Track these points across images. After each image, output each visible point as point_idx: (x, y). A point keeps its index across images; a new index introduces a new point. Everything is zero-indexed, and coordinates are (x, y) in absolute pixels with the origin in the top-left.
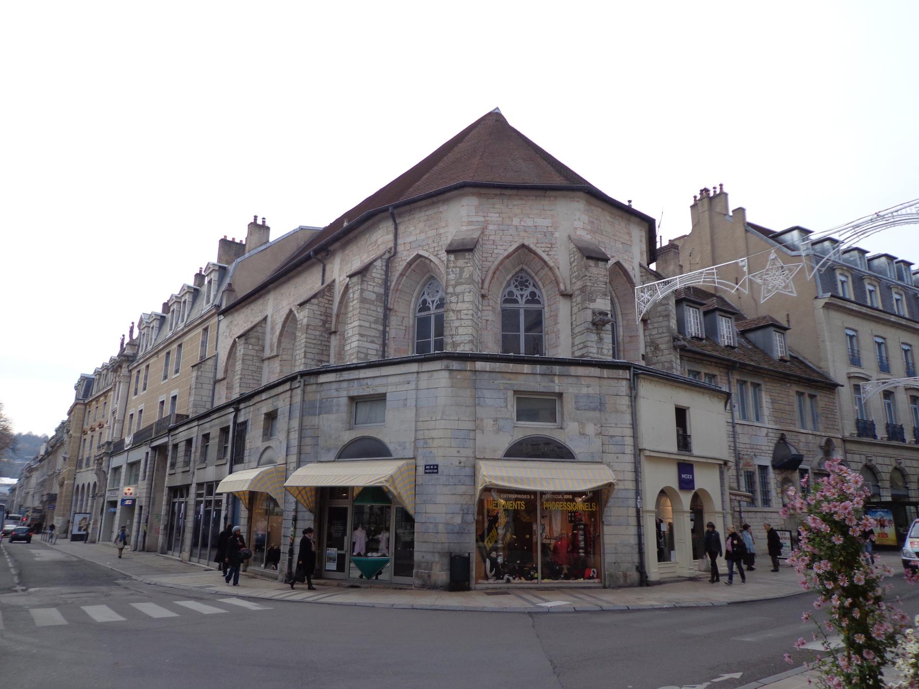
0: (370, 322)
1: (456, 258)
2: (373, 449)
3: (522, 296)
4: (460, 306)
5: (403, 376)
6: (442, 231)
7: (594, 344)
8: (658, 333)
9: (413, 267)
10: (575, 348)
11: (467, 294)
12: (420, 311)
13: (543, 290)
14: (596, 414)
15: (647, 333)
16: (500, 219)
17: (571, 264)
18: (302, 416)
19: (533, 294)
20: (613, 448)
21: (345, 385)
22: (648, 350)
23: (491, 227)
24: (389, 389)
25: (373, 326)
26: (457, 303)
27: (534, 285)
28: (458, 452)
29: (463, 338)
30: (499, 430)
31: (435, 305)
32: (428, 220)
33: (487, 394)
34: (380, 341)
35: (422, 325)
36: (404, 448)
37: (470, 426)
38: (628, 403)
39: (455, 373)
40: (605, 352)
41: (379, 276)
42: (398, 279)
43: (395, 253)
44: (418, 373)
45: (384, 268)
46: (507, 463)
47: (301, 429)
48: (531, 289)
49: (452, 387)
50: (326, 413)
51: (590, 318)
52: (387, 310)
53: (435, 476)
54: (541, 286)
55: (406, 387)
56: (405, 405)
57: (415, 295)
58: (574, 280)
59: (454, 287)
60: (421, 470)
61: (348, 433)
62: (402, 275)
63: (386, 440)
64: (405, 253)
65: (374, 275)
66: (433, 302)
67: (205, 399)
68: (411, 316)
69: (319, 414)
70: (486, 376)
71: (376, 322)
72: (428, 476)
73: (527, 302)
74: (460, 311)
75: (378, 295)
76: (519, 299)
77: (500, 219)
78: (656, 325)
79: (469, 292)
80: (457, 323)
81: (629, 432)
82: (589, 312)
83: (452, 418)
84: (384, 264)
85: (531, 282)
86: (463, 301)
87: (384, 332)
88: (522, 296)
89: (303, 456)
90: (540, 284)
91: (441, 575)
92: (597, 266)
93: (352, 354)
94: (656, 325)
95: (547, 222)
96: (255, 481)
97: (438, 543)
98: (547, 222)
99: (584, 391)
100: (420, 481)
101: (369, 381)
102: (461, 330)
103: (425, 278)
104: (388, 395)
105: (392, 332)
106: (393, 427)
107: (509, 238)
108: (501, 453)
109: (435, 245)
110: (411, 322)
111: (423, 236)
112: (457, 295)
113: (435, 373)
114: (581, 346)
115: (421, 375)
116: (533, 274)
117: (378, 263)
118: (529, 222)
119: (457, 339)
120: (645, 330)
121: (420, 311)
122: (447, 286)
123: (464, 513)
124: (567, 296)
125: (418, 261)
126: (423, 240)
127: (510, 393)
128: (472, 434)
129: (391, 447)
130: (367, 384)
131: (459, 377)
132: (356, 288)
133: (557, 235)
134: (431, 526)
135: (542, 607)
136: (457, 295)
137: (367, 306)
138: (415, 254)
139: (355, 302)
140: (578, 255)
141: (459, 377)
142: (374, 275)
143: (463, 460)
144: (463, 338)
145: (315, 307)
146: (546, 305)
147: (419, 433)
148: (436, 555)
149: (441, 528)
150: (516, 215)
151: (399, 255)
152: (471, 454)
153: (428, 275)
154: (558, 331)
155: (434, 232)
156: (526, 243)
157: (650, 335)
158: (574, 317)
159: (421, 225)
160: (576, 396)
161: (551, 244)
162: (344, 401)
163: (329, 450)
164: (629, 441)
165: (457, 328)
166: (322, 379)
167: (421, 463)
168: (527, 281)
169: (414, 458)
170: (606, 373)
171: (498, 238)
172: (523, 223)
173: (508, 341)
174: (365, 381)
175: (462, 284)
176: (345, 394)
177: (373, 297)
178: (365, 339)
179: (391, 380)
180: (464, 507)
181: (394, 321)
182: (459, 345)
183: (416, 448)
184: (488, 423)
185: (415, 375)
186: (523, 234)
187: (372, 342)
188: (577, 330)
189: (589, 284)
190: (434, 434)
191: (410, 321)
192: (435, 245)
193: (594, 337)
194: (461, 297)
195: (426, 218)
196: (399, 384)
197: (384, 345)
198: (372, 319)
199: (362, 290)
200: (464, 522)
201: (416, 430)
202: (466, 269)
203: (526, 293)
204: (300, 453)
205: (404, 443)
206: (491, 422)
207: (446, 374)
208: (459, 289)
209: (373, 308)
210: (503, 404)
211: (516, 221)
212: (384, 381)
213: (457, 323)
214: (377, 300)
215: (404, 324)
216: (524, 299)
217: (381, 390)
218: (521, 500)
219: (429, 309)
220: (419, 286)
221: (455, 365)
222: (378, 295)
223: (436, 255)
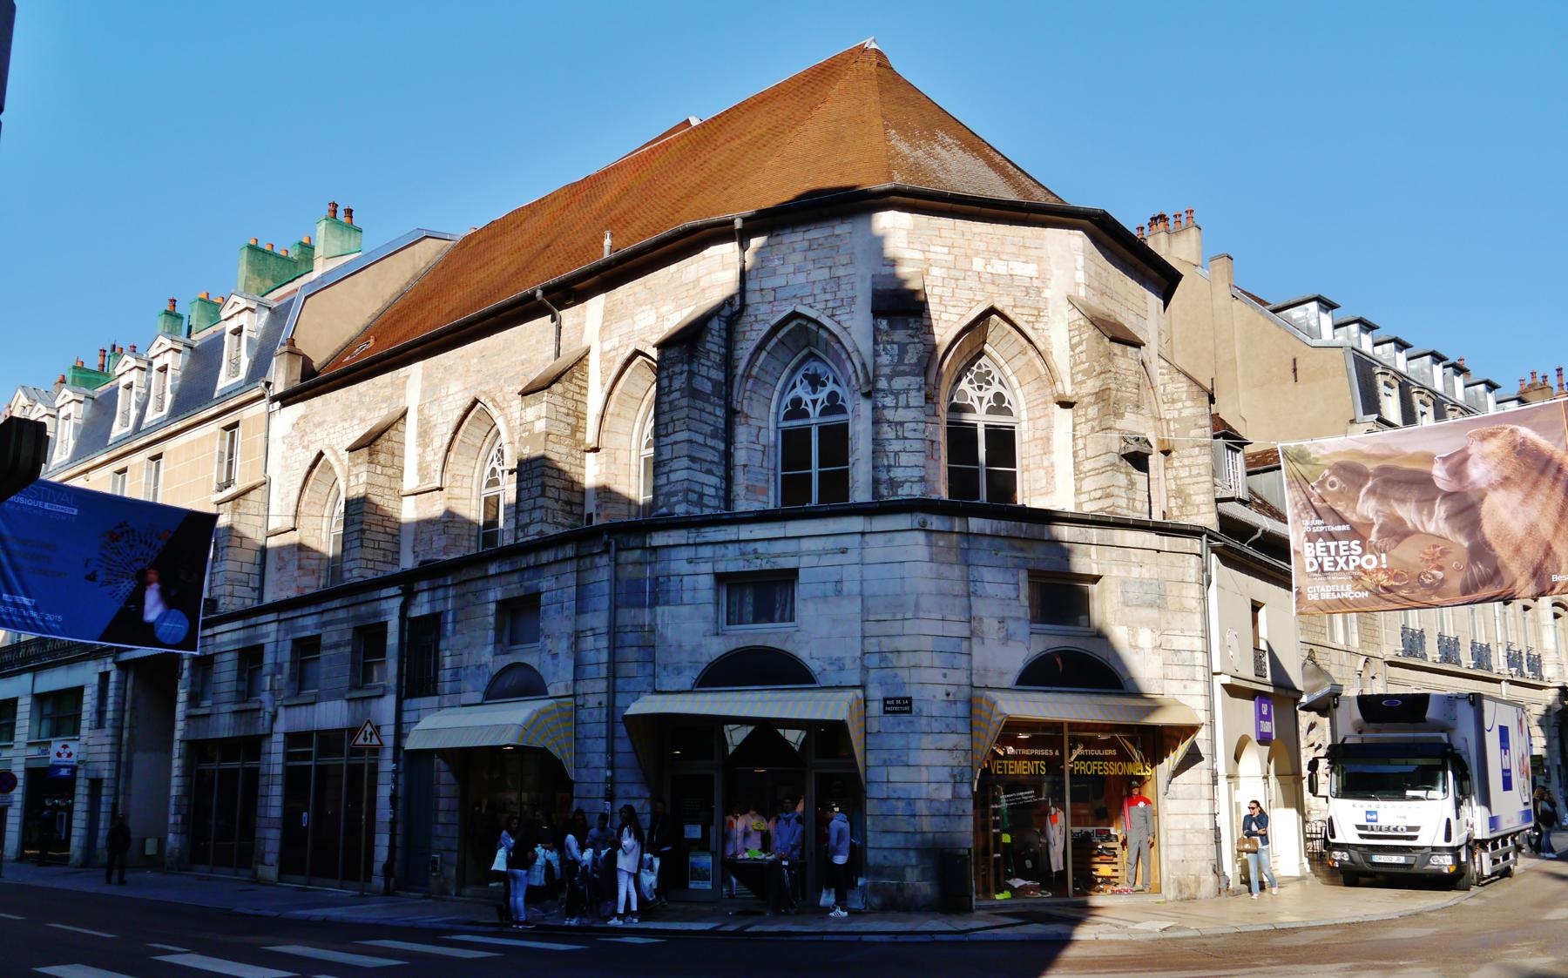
0: (706, 435)
1: (892, 326)
2: (783, 670)
3: (981, 399)
4: (901, 415)
5: (832, 539)
6: (841, 272)
7: (1122, 492)
8: (1190, 476)
9: (781, 334)
10: (1083, 498)
11: (913, 393)
12: (787, 417)
13: (1019, 392)
14: (1153, 613)
15: (1170, 474)
16: (951, 258)
17: (1073, 347)
18: (614, 608)
19: (999, 397)
20: (1177, 671)
21: (706, 552)
22: (1173, 503)
23: (935, 271)
24: (805, 561)
25: (710, 442)
26: (896, 408)
27: (1001, 382)
28: (945, 676)
29: (909, 472)
30: (1008, 638)
31: (818, 408)
32: (810, 248)
33: (988, 574)
34: (719, 471)
35: (793, 445)
36: (841, 669)
37: (960, 630)
38: (1198, 595)
39: (934, 537)
40: (1138, 505)
41: (715, 348)
42: (752, 355)
43: (743, 306)
44: (863, 534)
45: (724, 334)
46: (1019, 696)
47: (614, 631)
49: (931, 561)
50: (667, 603)
51: (1117, 446)
52: (732, 414)
53: (906, 717)
54: (1016, 385)
55: (840, 558)
56: (839, 593)
57: (779, 386)
58: (1079, 377)
59: (890, 378)
60: (875, 708)
61: (716, 640)
62: (760, 348)
63: (803, 655)
64: (764, 308)
65: (708, 346)
66: (814, 402)
68: (772, 426)
69: (654, 604)
70: (986, 542)
71: (714, 436)
72: (890, 719)
73: (990, 411)
74: (902, 424)
75: (715, 383)
76: (976, 405)
77: (951, 258)
78: (1186, 462)
79: (919, 390)
80: (896, 446)
81: (1198, 644)
82: (1115, 435)
83: (933, 616)
84: (723, 325)
85: (996, 373)
86: (908, 406)
87: (728, 456)
88: (981, 399)
89: (619, 682)
90: (1013, 379)
91: (919, 883)
92: (1125, 355)
93: (675, 494)
94: (1186, 462)
95: (1031, 270)
96: (527, 727)
97: (915, 833)
98: (1031, 270)
99: (1136, 572)
100: (874, 726)
101: (760, 547)
102: (904, 459)
103: (800, 356)
104: (801, 572)
105: (740, 456)
106: (812, 632)
107: (966, 294)
108: (1010, 679)
109: (828, 296)
110: (772, 438)
111: (801, 278)
112: (896, 394)
113: (897, 535)
114: (1099, 494)
115: (867, 538)
116: (1002, 362)
117: (715, 324)
118: (999, 267)
119: (898, 473)
120: (1166, 468)
121: (787, 417)
122: (876, 377)
123: (956, 780)
124: (1066, 404)
125: (793, 325)
126: (803, 286)
127: (1023, 575)
128: (965, 645)
129: (814, 666)
130: (755, 551)
131: (941, 543)
132: (677, 369)
133: (1047, 293)
134: (900, 804)
135: (1137, 932)
136: (896, 394)
137: (699, 404)
138: (789, 310)
139: (676, 395)
140: (1090, 333)
141: (941, 543)
142: (708, 346)
143: (952, 689)
144: (909, 472)
145: (558, 400)
146: (1024, 415)
147: (866, 641)
148: (912, 854)
149: (921, 807)
150: (977, 253)
151: (750, 310)
152: (965, 681)
153: (805, 352)
154: (1052, 465)
155: (825, 274)
156: (999, 306)
157: (1175, 478)
158: (1080, 443)
159: (797, 258)
160: (1124, 582)
161: (1039, 310)
162: (706, 582)
163: (679, 671)
164: (1200, 658)
165: (896, 453)
166: (659, 539)
167: (876, 693)
168: (989, 373)
169: (862, 687)
170: (1167, 542)
171: (947, 293)
172: (989, 269)
173: (962, 481)
174: (752, 546)
175: (903, 374)
176: (707, 568)
177: (707, 387)
178: (697, 466)
179: (806, 544)
180: (956, 771)
181: (742, 434)
182: (901, 484)
183: (865, 669)
184: (990, 626)
185: (858, 537)
186: (990, 288)
187: (709, 472)
188: (1087, 466)
189: (1113, 386)
190: (901, 644)
191: (771, 436)
192: (828, 296)
193: (1122, 480)
194: (902, 398)
195: (806, 244)
196: (826, 552)
197: (728, 479)
198: (708, 429)
199: (691, 374)
200: (956, 796)
201: (864, 637)
202: (910, 348)
203: (988, 394)
204: (612, 676)
205: (839, 659)
206: (995, 624)
207: (920, 537)
208: (898, 383)
209: (709, 408)
210: (1013, 594)
211: (978, 264)
212: (791, 546)
213: (896, 446)
214: (714, 393)
215: (763, 440)
216: (985, 406)
217: (788, 563)
218: (1039, 758)
219: (806, 415)
220: (787, 371)
221: (935, 522)
222: (715, 383)
223: (832, 316)
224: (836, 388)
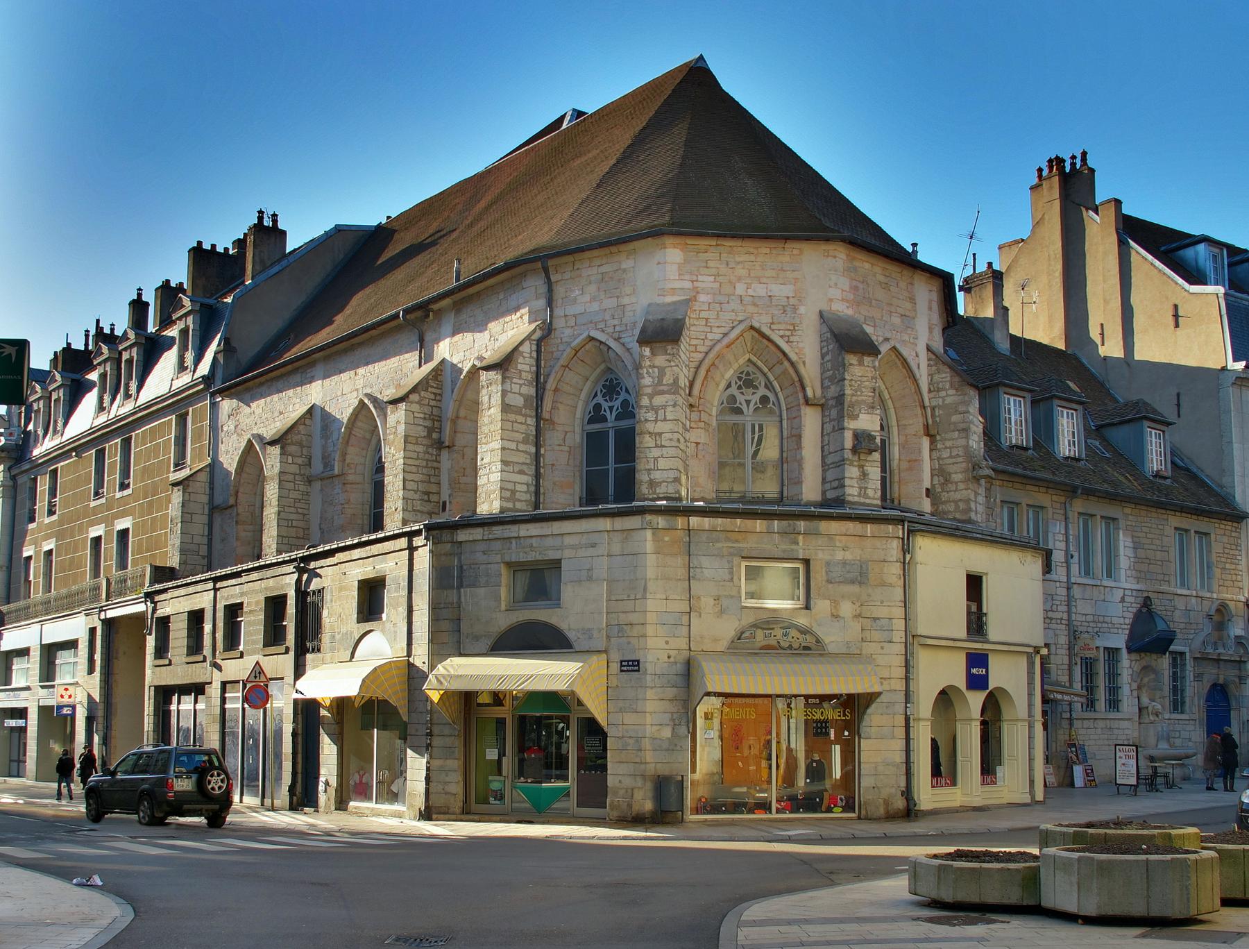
0: (518, 442)
1: (653, 353)
4: (660, 427)
6: (626, 301)
7: (854, 483)
8: (951, 457)
10: (828, 486)
12: (590, 421)
14: (854, 589)
15: (935, 454)
16: (716, 285)
20: (877, 635)
21: (498, 545)
22: (935, 482)
23: (702, 298)
24: (567, 553)
25: (522, 447)
26: (656, 421)
28: (667, 643)
29: (665, 475)
33: (705, 561)
35: (595, 444)
40: (870, 493)
41: (527, 368)
45: (534, 355)
48: (762, 391)
55: (590, 551)
57: (583, 396)
58: (827, 383)
59: (651, 397)
63: (563, 626)
65: (520, 366)
66: (611, 408)
67: (197, 540)
68: (578, 429)
69: (460, 586)
71: (525, 441)
74: (660, 434)
76: (744, 408)
77: (716, 285)
78: (948, 444)
80: (656, 452)
81: (899, 612)
83: (658, 596)
84: (534, 347)
86: (665, 420)
87: (537, 456)
88: (748, 402)
92: (861, 363)
94: (948, 444)
95: (787, 290)
98: (787, 290)
99: (840, 555)
102: (662, 464)
103: (598, 371)
105: (548, 457)
106: (574, 609)
111: (595, 306)
114: (835, 484)
117: (526, 348)
118: (760, 290)
119: (657, 476)
120: (931, 450)
121: (590, 421)
129: (571, 636)
130: (531, 546)
132: (493, 388)
133: (802, 310)
134: (631, 741)
136: (656, 410)
137: (512, 417)
141: (667, 539)
142: (520, 366)
143: (673, 653)
145: (415, 407)
150: (740, 279)
157: (939, 459)
158: (826, 438)
159: (592, 288)
160: (828, 564)
161: (794, 325)
164: (900, 624)
165: (656, 459)
166: (462, 535)
171: (712, 315)
172: (750, 292)
174: (529, 541)
175: (663, 393)
177: (519, 401)
178: (510, 468)
181: (553, 439)
184: (707, 603)
186: (751, 309)
187: (521, 472)
188: (829, 460)
192: (616, 322)
194: (661, 413)
195: (600, 276)
199: (504, 393)
200: (674, 735)
205: (589, 630)
206: (712, 602)
208: (659, 400)
209: (520, 419)
210: (727, 577)
211: (740, 289)
212: (557, 542)
213: (656, 452)
214: (525, 406)
219: (604, 419)
220: (589, 384)
223: (617, 339)
224: (627, 397)
